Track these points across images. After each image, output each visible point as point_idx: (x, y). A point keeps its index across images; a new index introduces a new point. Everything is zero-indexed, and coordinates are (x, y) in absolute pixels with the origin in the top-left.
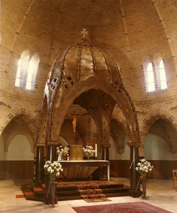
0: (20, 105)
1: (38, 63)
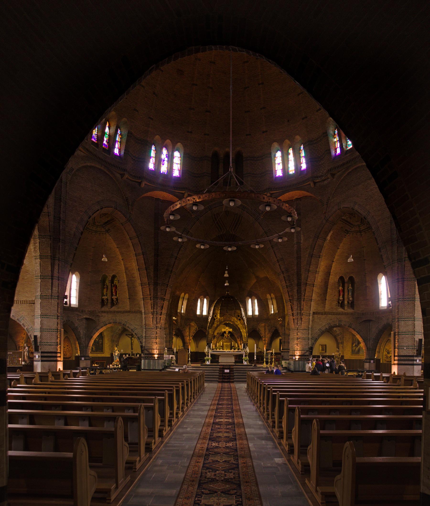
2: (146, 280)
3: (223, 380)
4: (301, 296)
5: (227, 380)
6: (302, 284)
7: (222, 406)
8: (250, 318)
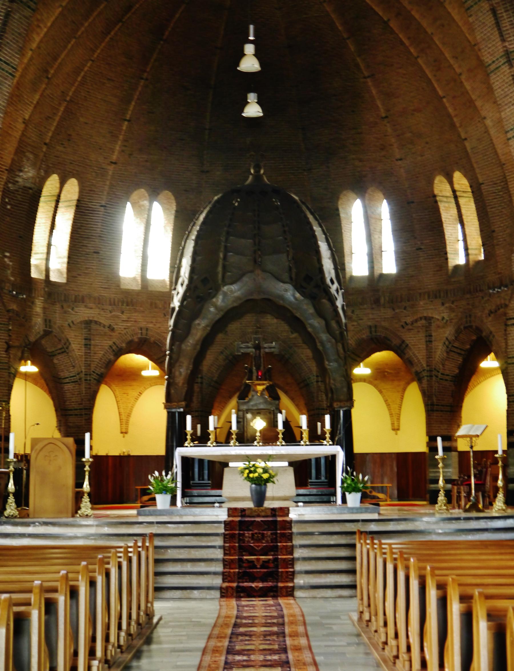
0: (135, 321)
1: (173, 212)
3: (246, 584)
5: (260, 585)
8: (359, 292)
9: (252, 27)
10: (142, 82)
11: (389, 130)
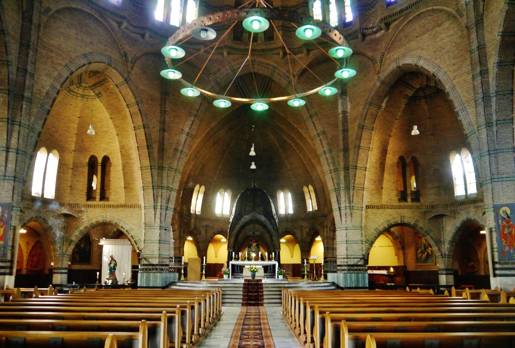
2: (147, 162)
3: (249, 302)
4: (350, 183)
5: (253, 302)
6: (350, 167)
7: (248, 327)
9: (253, 144)
10: (223, 160)
11: (291, 173)
